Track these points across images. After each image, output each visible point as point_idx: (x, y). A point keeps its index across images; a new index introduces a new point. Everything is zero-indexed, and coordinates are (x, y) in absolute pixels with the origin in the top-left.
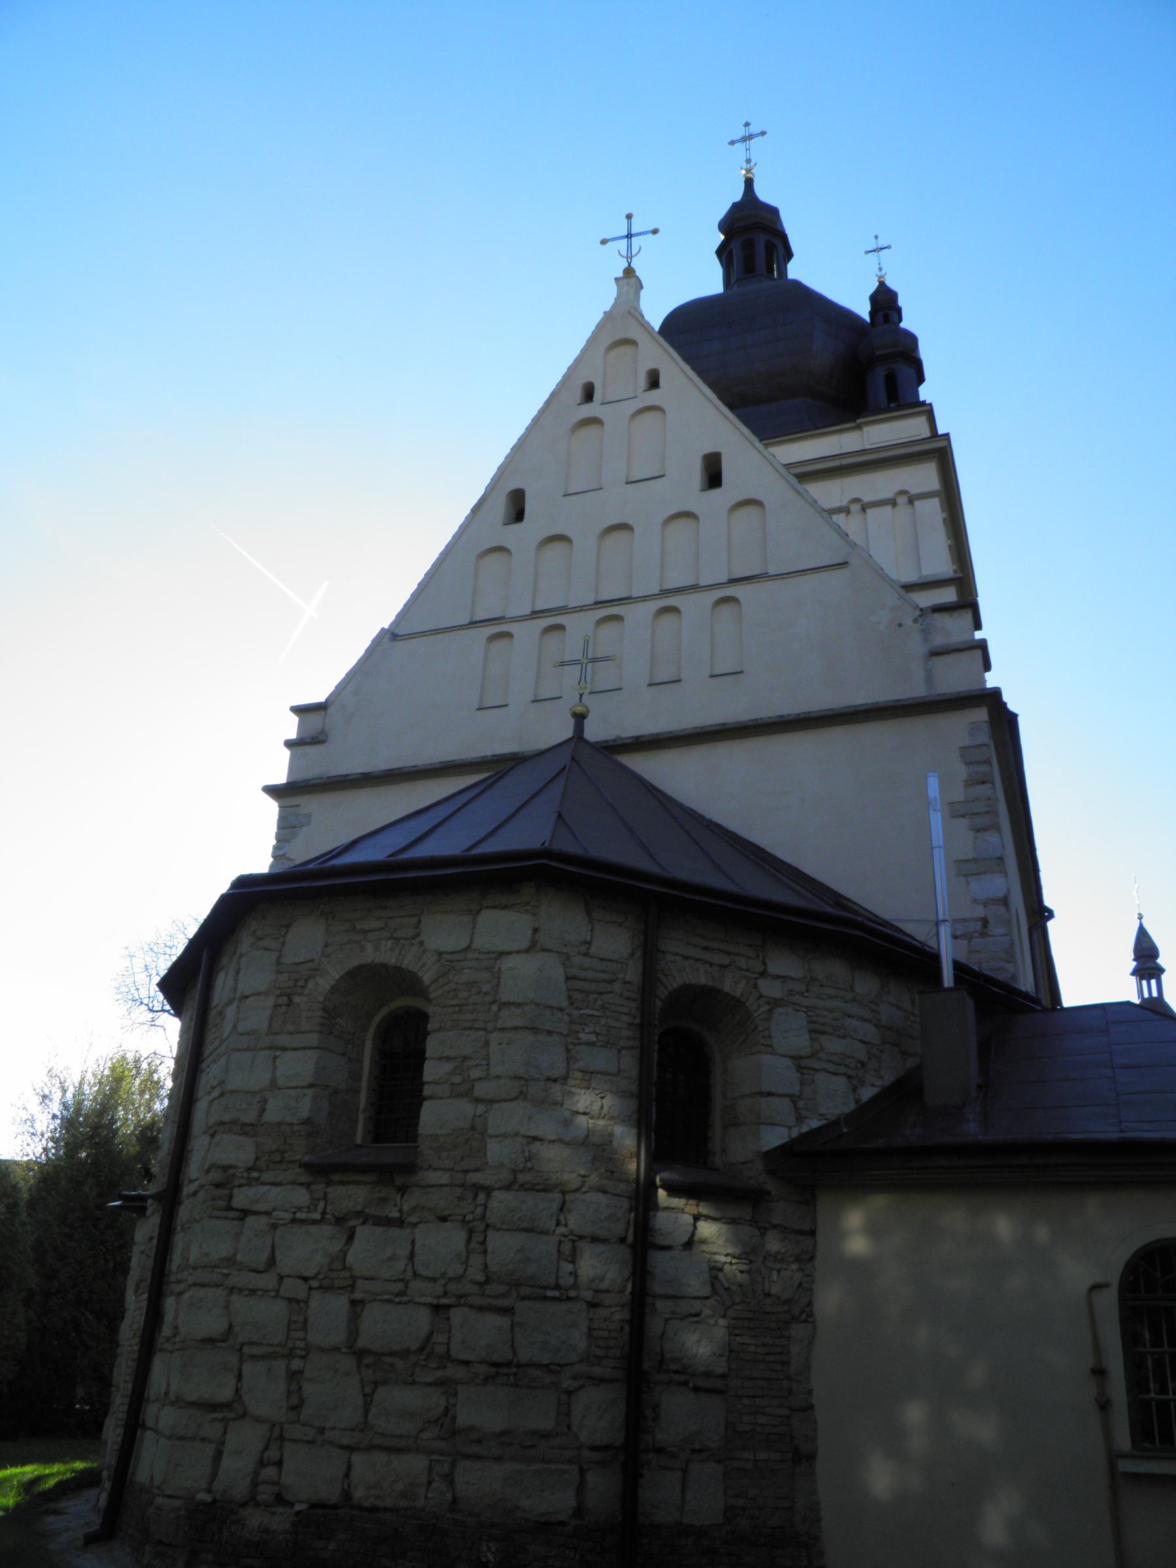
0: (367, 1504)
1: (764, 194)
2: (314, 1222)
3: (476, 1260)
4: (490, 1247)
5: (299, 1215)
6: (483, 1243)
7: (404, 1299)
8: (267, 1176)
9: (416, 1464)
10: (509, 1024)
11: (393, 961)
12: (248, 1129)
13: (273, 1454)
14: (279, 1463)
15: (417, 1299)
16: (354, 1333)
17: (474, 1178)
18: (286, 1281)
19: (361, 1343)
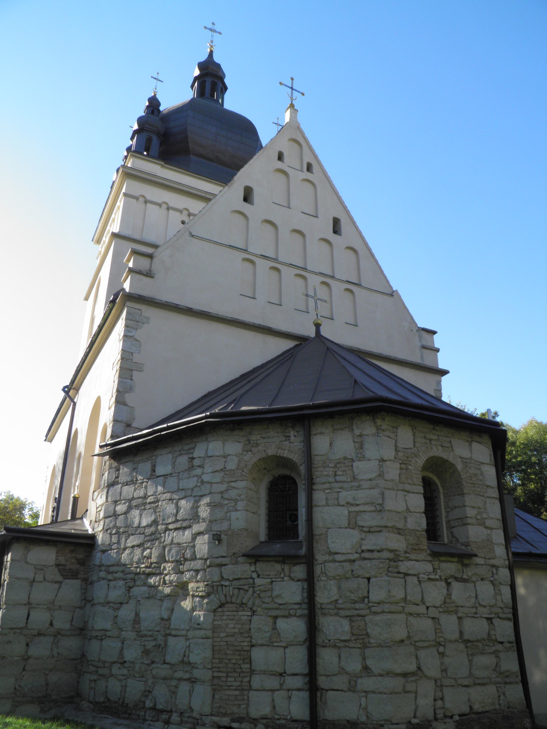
0: (480, 711)
1: (217, 58)
2: (437, 580)
3: (499, 598)
4: (503, 592)
5: (431, 577)
6: (499, 590)
7: (478, 616)
8: (413, 556)
9: (492, 689)
10: (491, 496)
11: (445, 457)
12: (401, 531)
13: (439, 694)
14: (442, 699)
15: (483, 616)
16: (461, 633)
17: (493, 562)
18: (430, 609)
19: (466, 637)
